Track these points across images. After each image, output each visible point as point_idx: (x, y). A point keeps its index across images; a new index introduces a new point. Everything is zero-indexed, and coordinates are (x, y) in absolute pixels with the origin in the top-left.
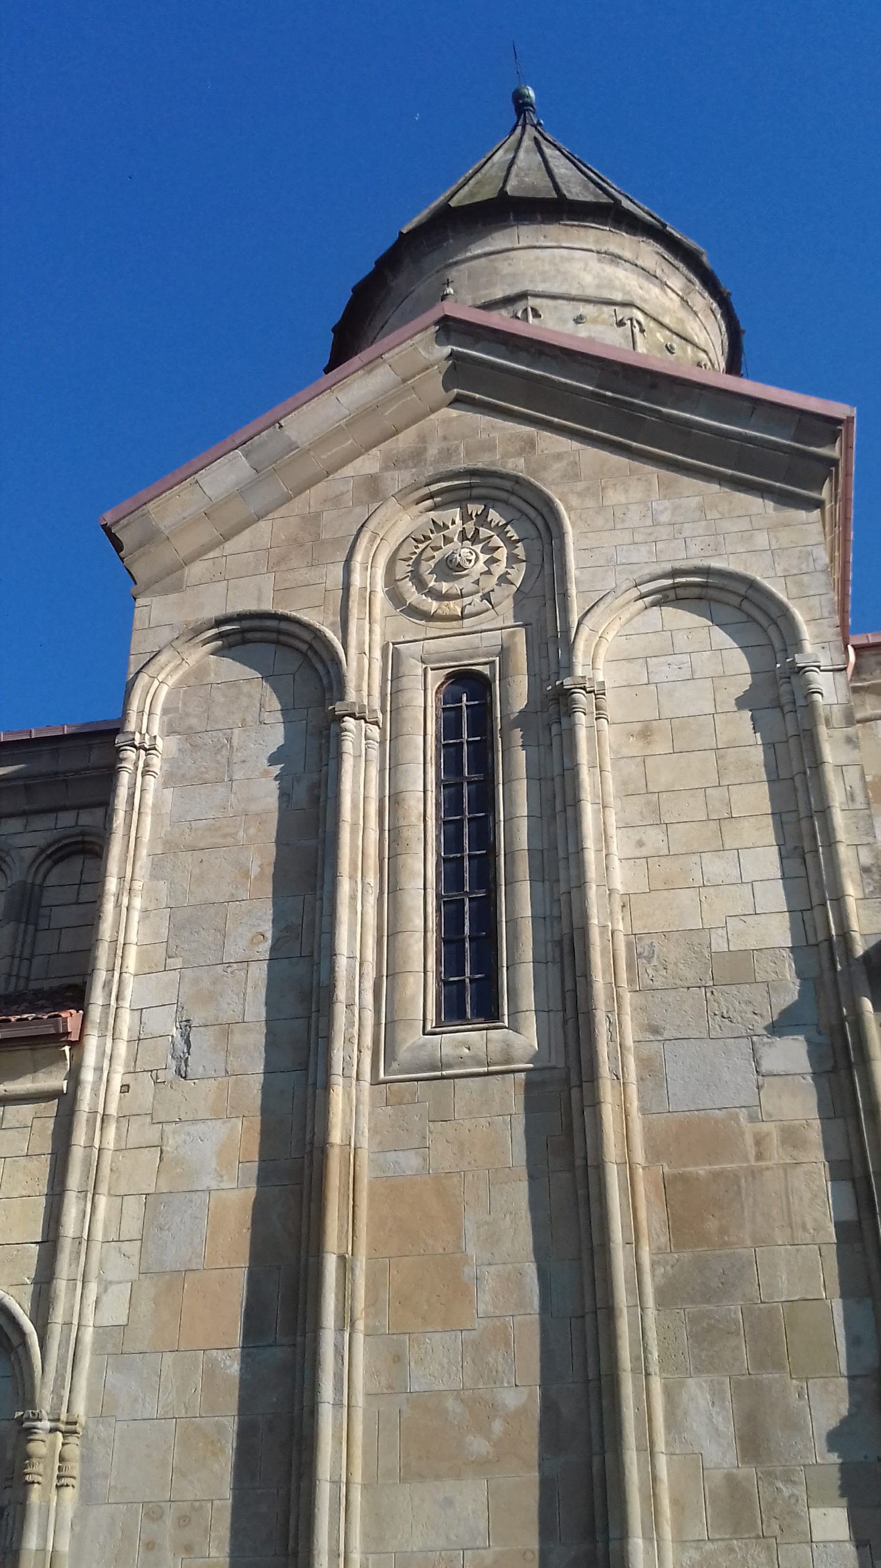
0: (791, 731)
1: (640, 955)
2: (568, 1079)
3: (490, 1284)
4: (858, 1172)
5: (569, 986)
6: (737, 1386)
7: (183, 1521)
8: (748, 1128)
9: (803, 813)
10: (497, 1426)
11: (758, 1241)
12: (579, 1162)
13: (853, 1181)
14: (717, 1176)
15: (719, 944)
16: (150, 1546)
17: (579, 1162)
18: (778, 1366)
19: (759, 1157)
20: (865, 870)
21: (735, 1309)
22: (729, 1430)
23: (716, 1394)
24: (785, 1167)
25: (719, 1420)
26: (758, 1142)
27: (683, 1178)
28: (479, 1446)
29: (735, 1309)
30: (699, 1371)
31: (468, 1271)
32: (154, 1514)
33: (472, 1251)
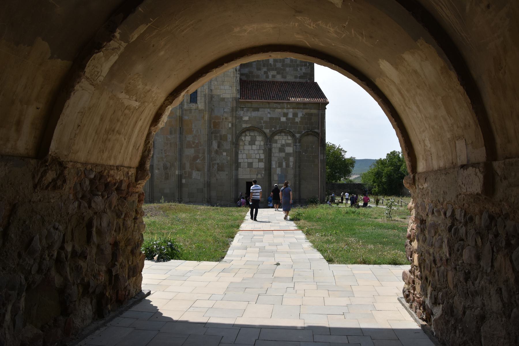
0: (233, 71)
1: (213, 97)
2: (204, 110)
3: (195, 131)
4: (232, 122)
5: (205, 100)
6: (218, 142)
7: (165, 151)
8: (222, 117)
9: (232, 82)
10: (195, 144)
11: (222, 128)
12: (205, 119)
13: (231, 123)
14: (218, 122)
15: (221, 97)
16: (162, 153)
17: (205, 119)
18: (222, 140)
19: (223, 120)
20: (238, 90)
21: (219, 135)
22: (217, 146)
23: (216, 142)
24: (225, 121)
25: (216, 145)
26: (223, 119)
27: (215, 122)
28: (193, 146)
29: (219, 135)
30: (214, 140)
31: (193, 129)
32: (162, 150)
33: (193, 127)
